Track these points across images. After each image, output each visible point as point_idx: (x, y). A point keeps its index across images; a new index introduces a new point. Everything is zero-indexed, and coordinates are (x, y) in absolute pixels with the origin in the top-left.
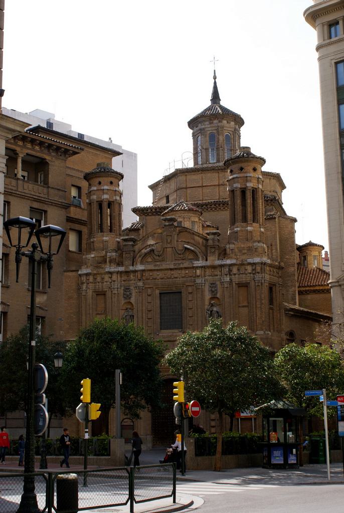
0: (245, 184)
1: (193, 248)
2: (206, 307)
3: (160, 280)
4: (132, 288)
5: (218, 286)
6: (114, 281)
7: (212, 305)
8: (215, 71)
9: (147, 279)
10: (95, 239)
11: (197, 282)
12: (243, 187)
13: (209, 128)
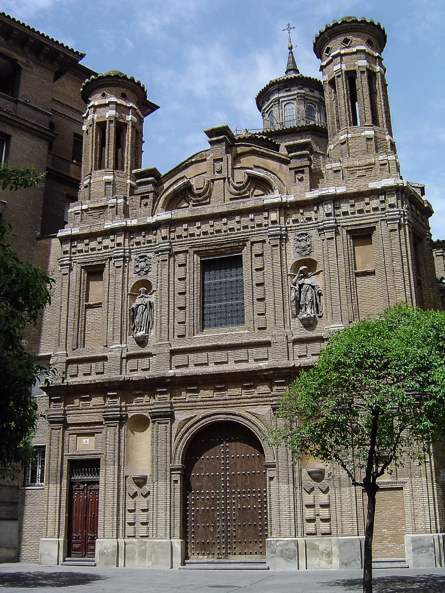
1: (262, 175)
13: (285, 97)
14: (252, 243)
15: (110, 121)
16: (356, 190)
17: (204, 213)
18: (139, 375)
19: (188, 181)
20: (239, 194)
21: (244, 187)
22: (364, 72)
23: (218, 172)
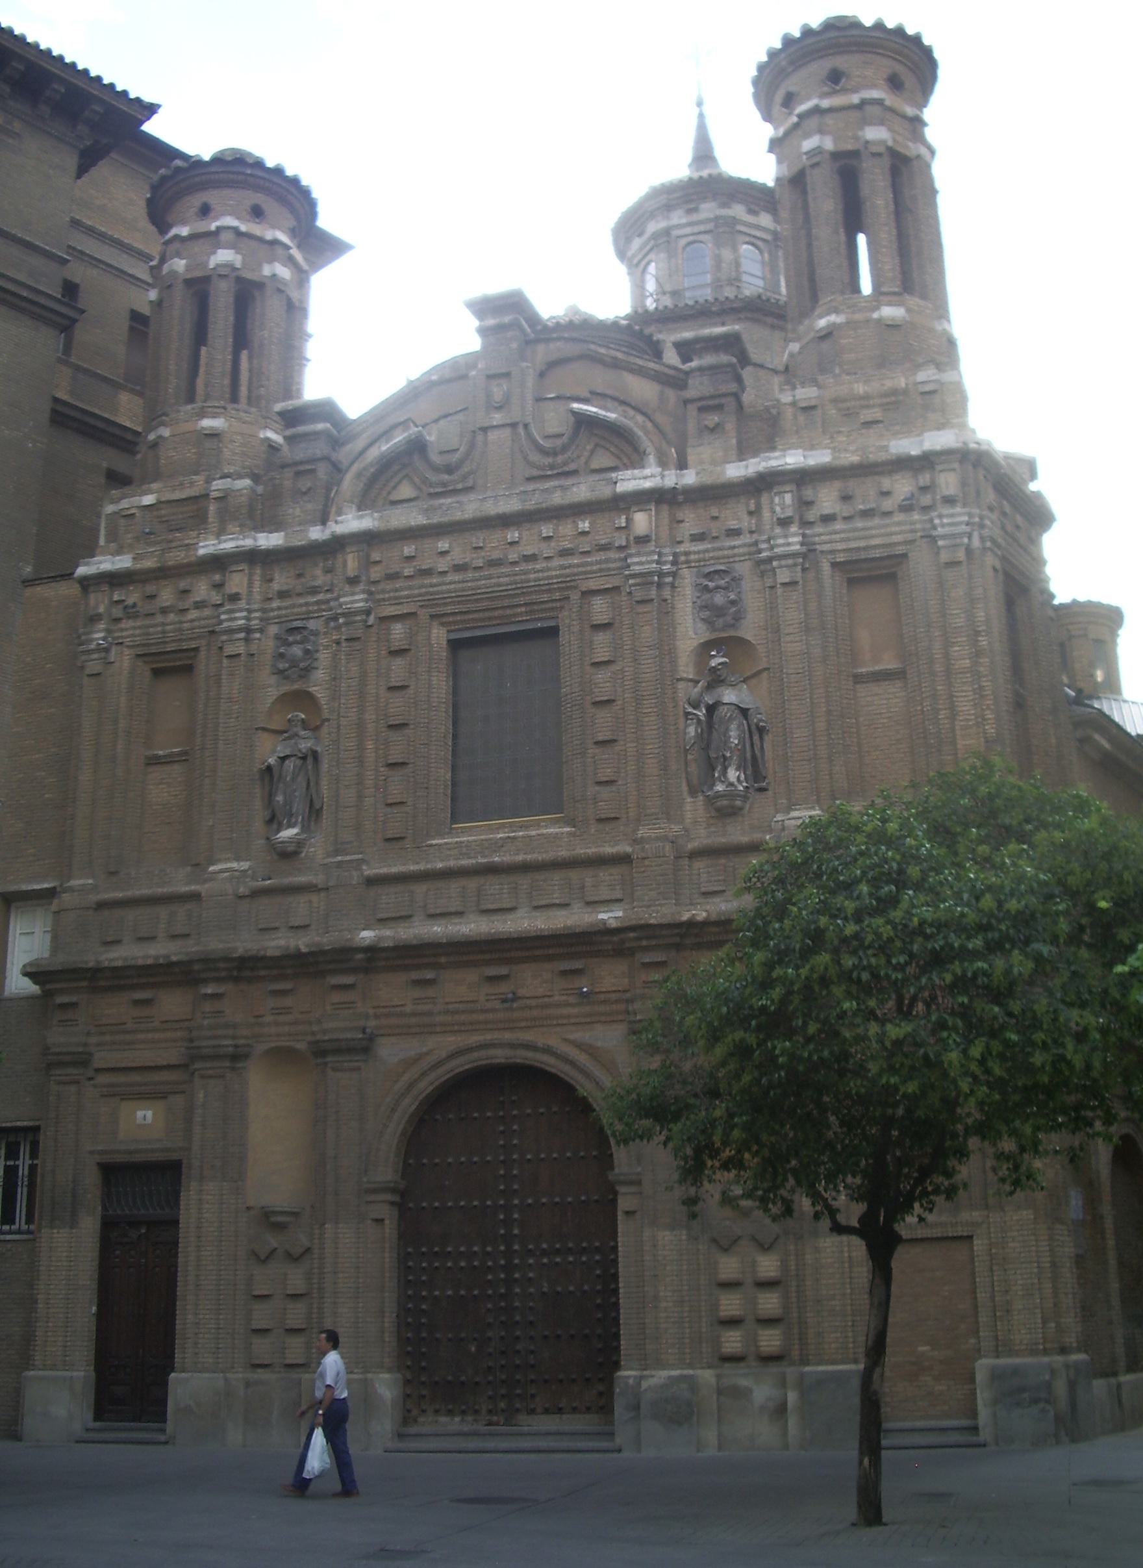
0: (856, 138)
1: (612, 416)
2: (684, 691)
5: (746, 585)
6: (234, 598)
7: (716, 680)
9: (392, 577)
10: (166, 432)
12: (850, 147)
14: (588, 594)
15: (220, 276)
16: (855, 459)
17: (458, 516)
18: (282, 942)
19: (420, 432)
20: (552, 467)
21: (565, 448)
22: (879, 155)
23: (499, 408)
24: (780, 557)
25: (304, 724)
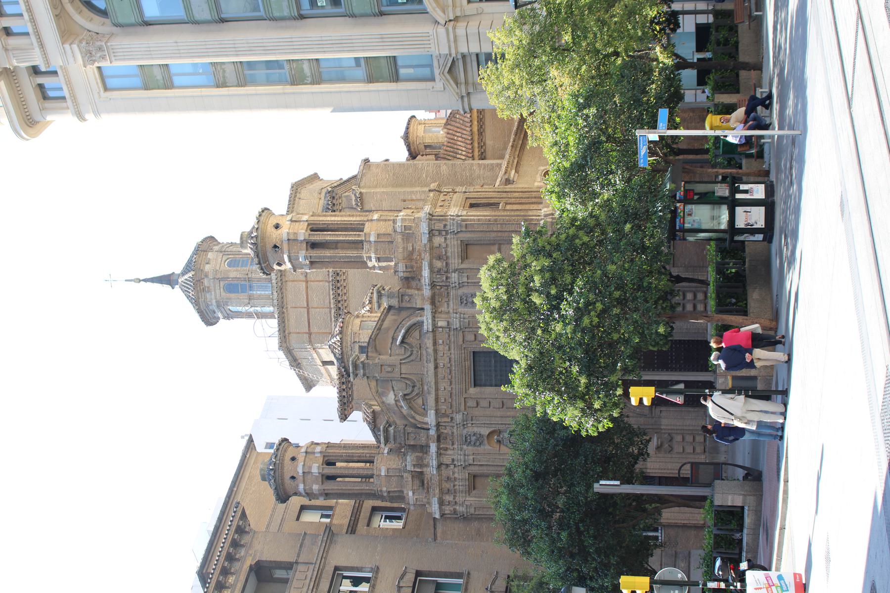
1: (403, 331)
3: (454, 386)
4: (465, 432)
6: (453, 460)
8: (126, 281)
11: (458, 326)
12: (305, 245)
13: (215, 293)
24: (459, 280)
25: (499, 436)
